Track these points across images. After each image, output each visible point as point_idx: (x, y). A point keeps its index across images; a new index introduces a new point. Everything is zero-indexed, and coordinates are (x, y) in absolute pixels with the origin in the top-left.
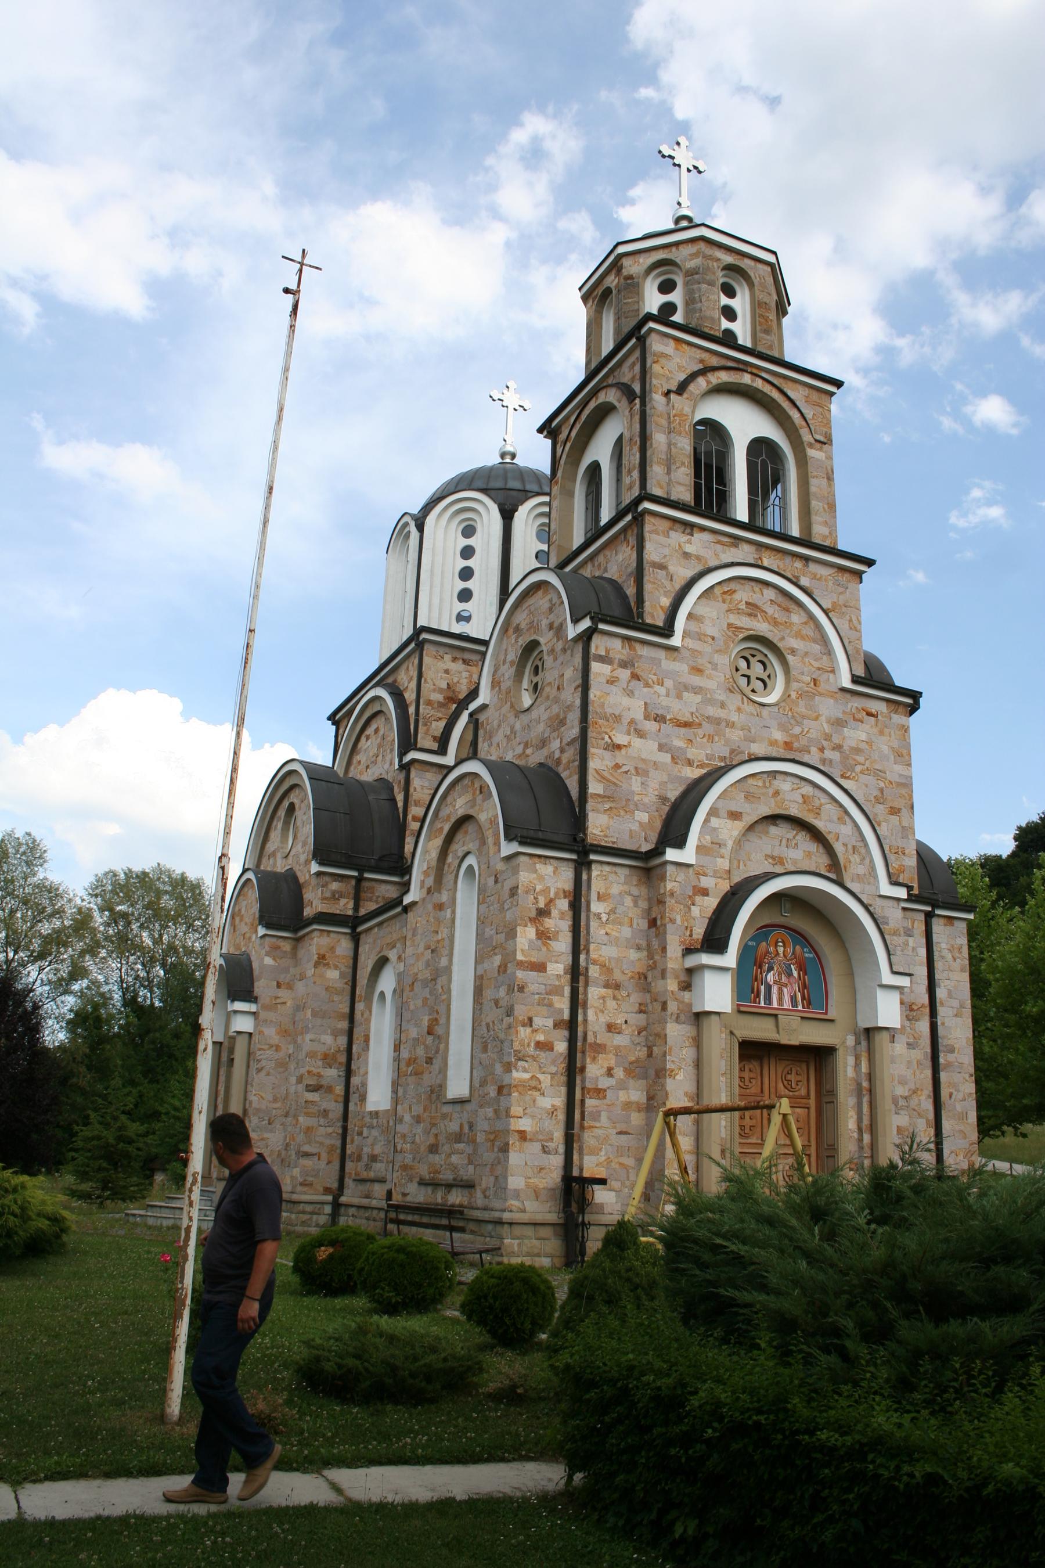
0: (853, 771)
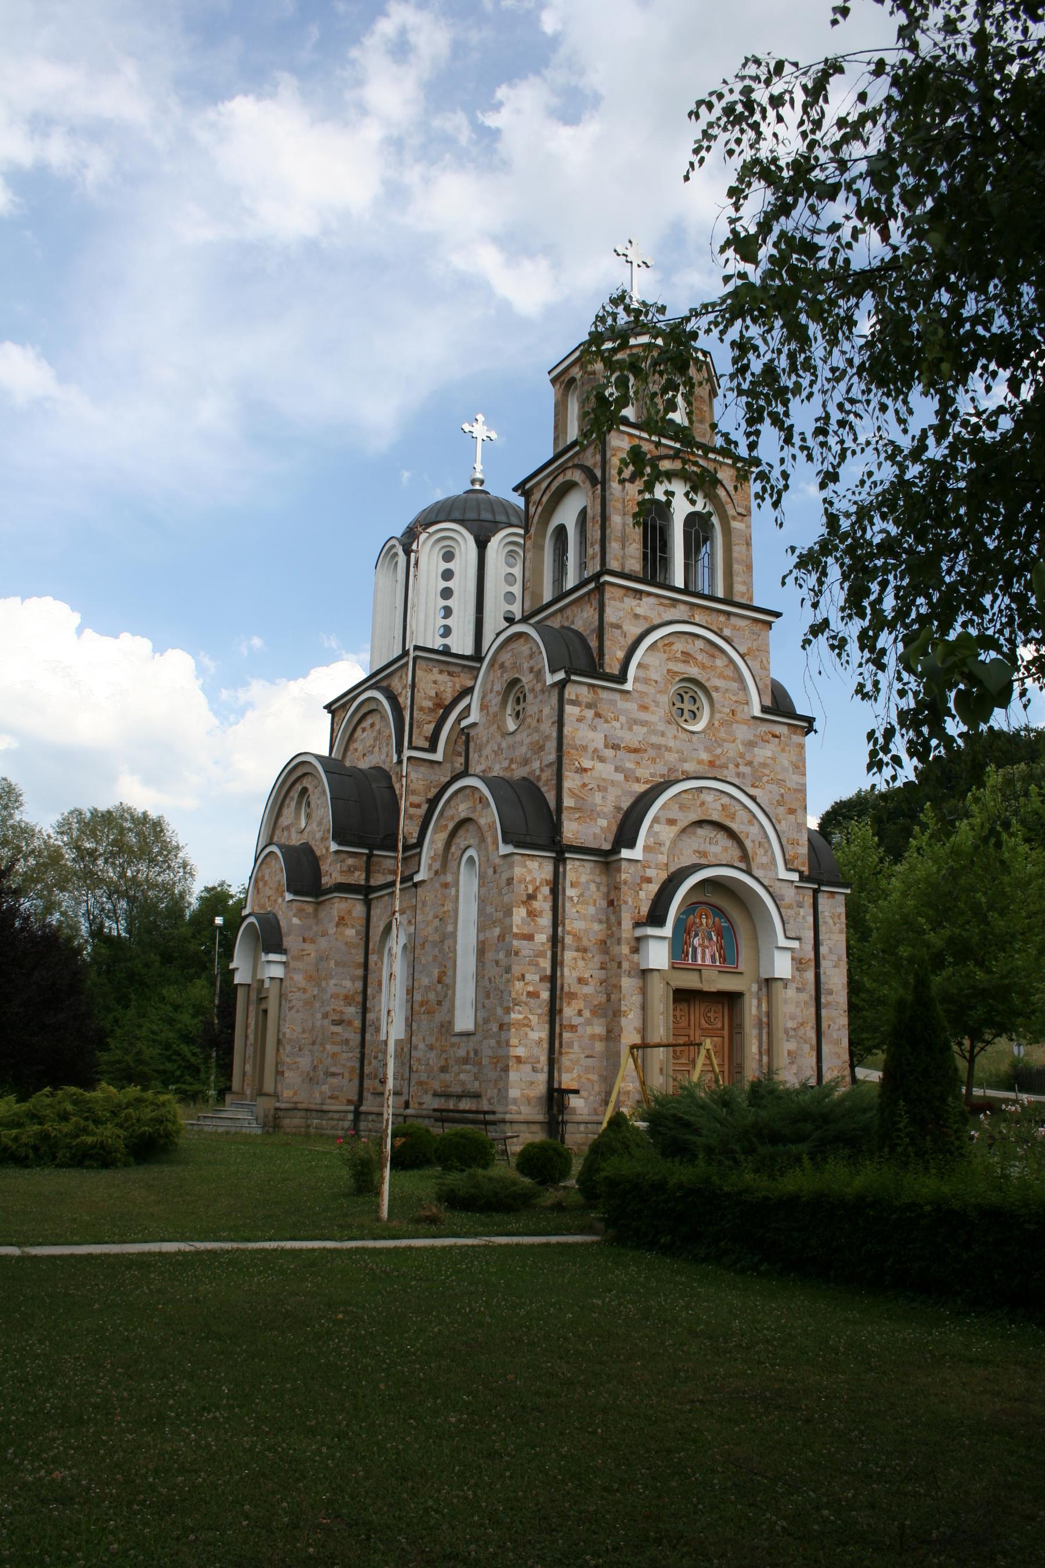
0: (761, 781)
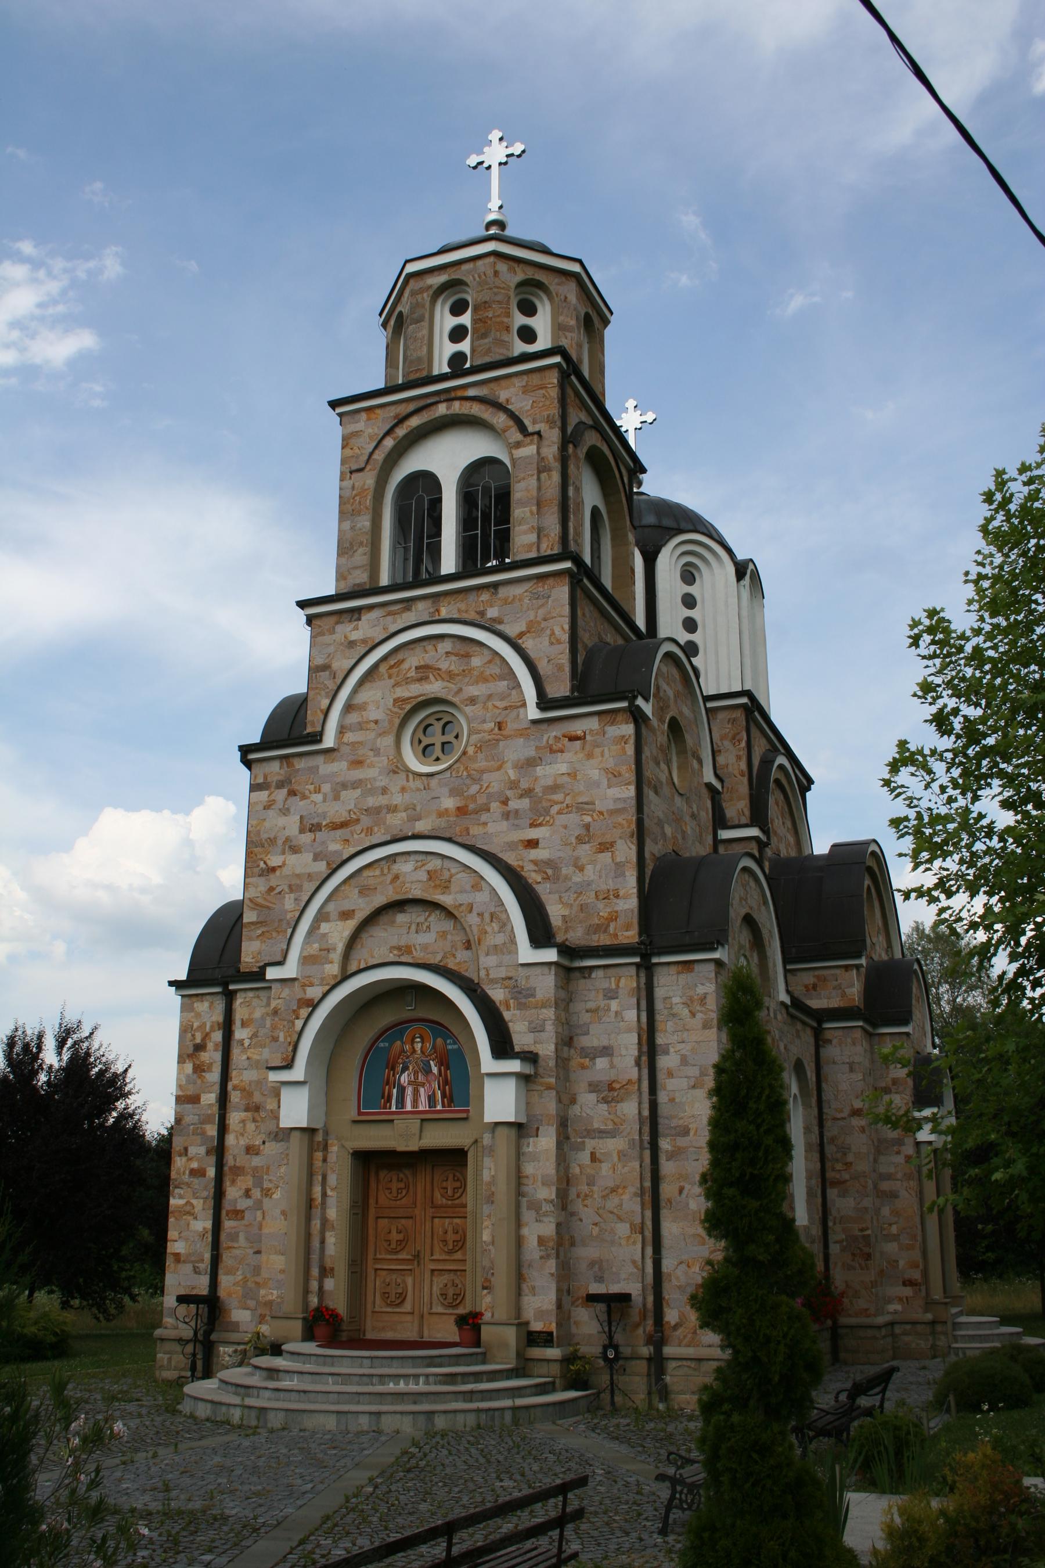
0: (547, 811)
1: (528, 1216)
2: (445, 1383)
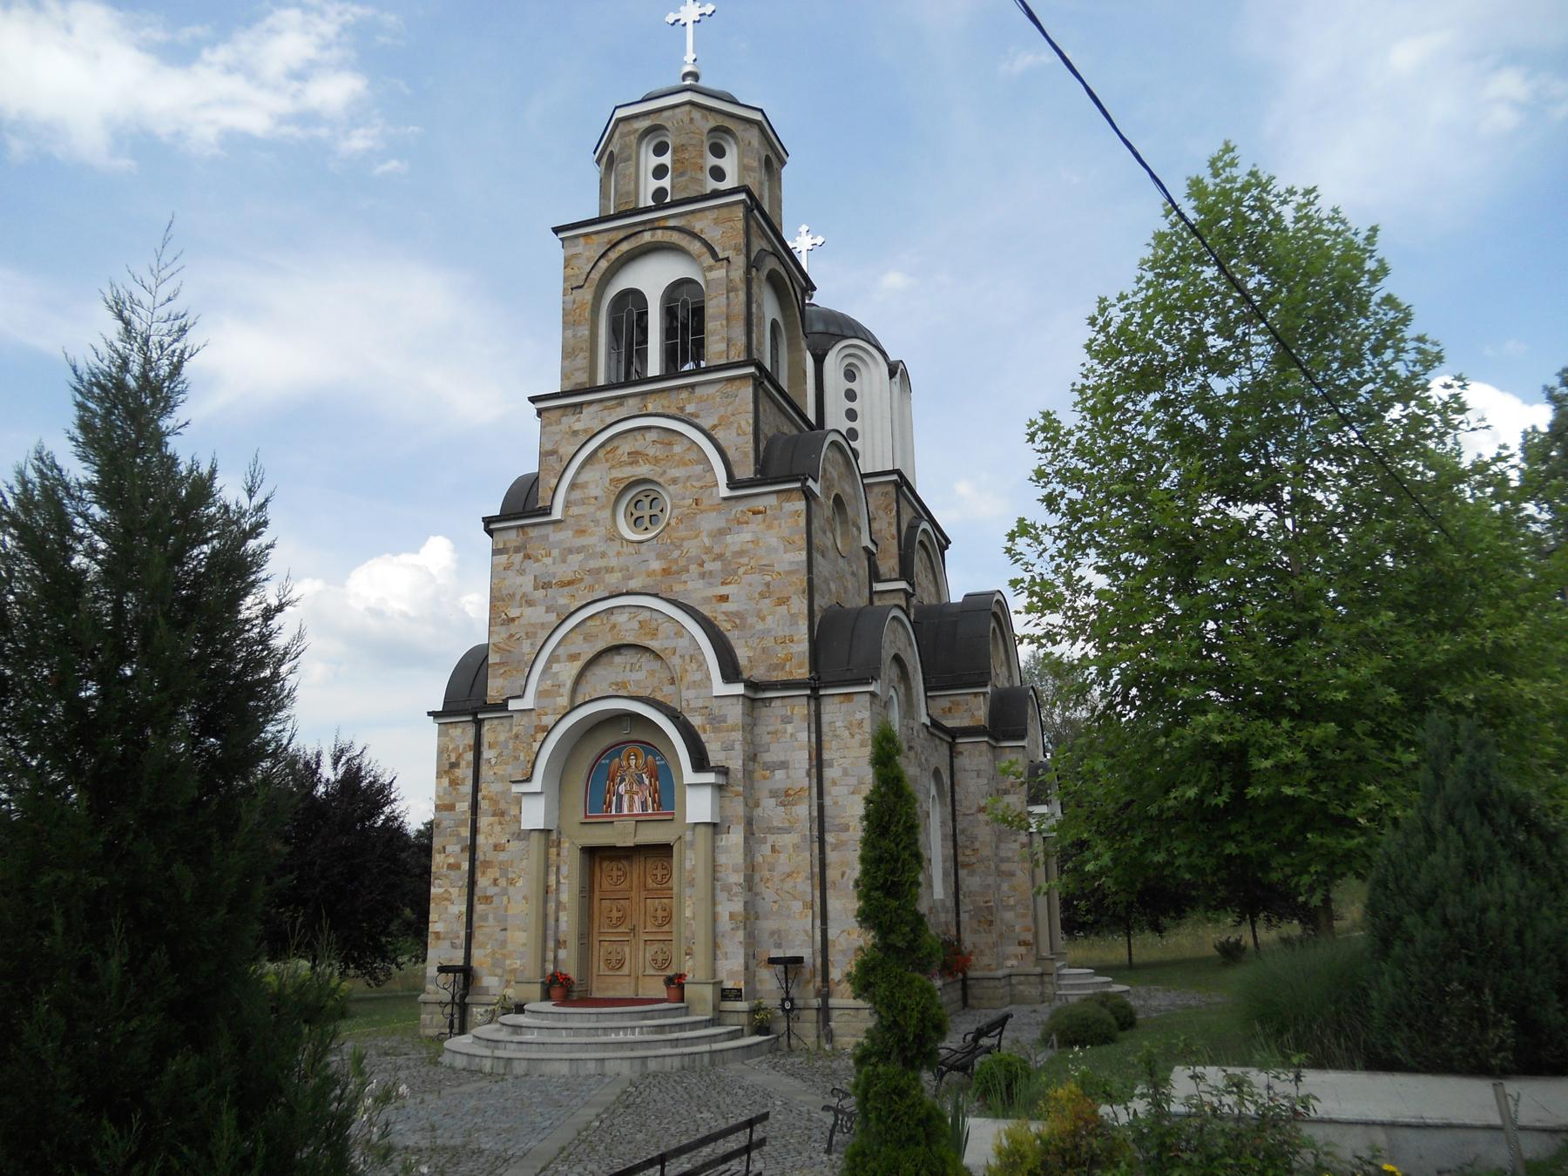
0: (735, 572)
1: (722, 896)
2: (656, 1033)
